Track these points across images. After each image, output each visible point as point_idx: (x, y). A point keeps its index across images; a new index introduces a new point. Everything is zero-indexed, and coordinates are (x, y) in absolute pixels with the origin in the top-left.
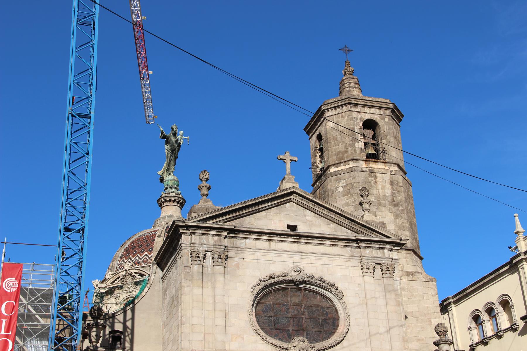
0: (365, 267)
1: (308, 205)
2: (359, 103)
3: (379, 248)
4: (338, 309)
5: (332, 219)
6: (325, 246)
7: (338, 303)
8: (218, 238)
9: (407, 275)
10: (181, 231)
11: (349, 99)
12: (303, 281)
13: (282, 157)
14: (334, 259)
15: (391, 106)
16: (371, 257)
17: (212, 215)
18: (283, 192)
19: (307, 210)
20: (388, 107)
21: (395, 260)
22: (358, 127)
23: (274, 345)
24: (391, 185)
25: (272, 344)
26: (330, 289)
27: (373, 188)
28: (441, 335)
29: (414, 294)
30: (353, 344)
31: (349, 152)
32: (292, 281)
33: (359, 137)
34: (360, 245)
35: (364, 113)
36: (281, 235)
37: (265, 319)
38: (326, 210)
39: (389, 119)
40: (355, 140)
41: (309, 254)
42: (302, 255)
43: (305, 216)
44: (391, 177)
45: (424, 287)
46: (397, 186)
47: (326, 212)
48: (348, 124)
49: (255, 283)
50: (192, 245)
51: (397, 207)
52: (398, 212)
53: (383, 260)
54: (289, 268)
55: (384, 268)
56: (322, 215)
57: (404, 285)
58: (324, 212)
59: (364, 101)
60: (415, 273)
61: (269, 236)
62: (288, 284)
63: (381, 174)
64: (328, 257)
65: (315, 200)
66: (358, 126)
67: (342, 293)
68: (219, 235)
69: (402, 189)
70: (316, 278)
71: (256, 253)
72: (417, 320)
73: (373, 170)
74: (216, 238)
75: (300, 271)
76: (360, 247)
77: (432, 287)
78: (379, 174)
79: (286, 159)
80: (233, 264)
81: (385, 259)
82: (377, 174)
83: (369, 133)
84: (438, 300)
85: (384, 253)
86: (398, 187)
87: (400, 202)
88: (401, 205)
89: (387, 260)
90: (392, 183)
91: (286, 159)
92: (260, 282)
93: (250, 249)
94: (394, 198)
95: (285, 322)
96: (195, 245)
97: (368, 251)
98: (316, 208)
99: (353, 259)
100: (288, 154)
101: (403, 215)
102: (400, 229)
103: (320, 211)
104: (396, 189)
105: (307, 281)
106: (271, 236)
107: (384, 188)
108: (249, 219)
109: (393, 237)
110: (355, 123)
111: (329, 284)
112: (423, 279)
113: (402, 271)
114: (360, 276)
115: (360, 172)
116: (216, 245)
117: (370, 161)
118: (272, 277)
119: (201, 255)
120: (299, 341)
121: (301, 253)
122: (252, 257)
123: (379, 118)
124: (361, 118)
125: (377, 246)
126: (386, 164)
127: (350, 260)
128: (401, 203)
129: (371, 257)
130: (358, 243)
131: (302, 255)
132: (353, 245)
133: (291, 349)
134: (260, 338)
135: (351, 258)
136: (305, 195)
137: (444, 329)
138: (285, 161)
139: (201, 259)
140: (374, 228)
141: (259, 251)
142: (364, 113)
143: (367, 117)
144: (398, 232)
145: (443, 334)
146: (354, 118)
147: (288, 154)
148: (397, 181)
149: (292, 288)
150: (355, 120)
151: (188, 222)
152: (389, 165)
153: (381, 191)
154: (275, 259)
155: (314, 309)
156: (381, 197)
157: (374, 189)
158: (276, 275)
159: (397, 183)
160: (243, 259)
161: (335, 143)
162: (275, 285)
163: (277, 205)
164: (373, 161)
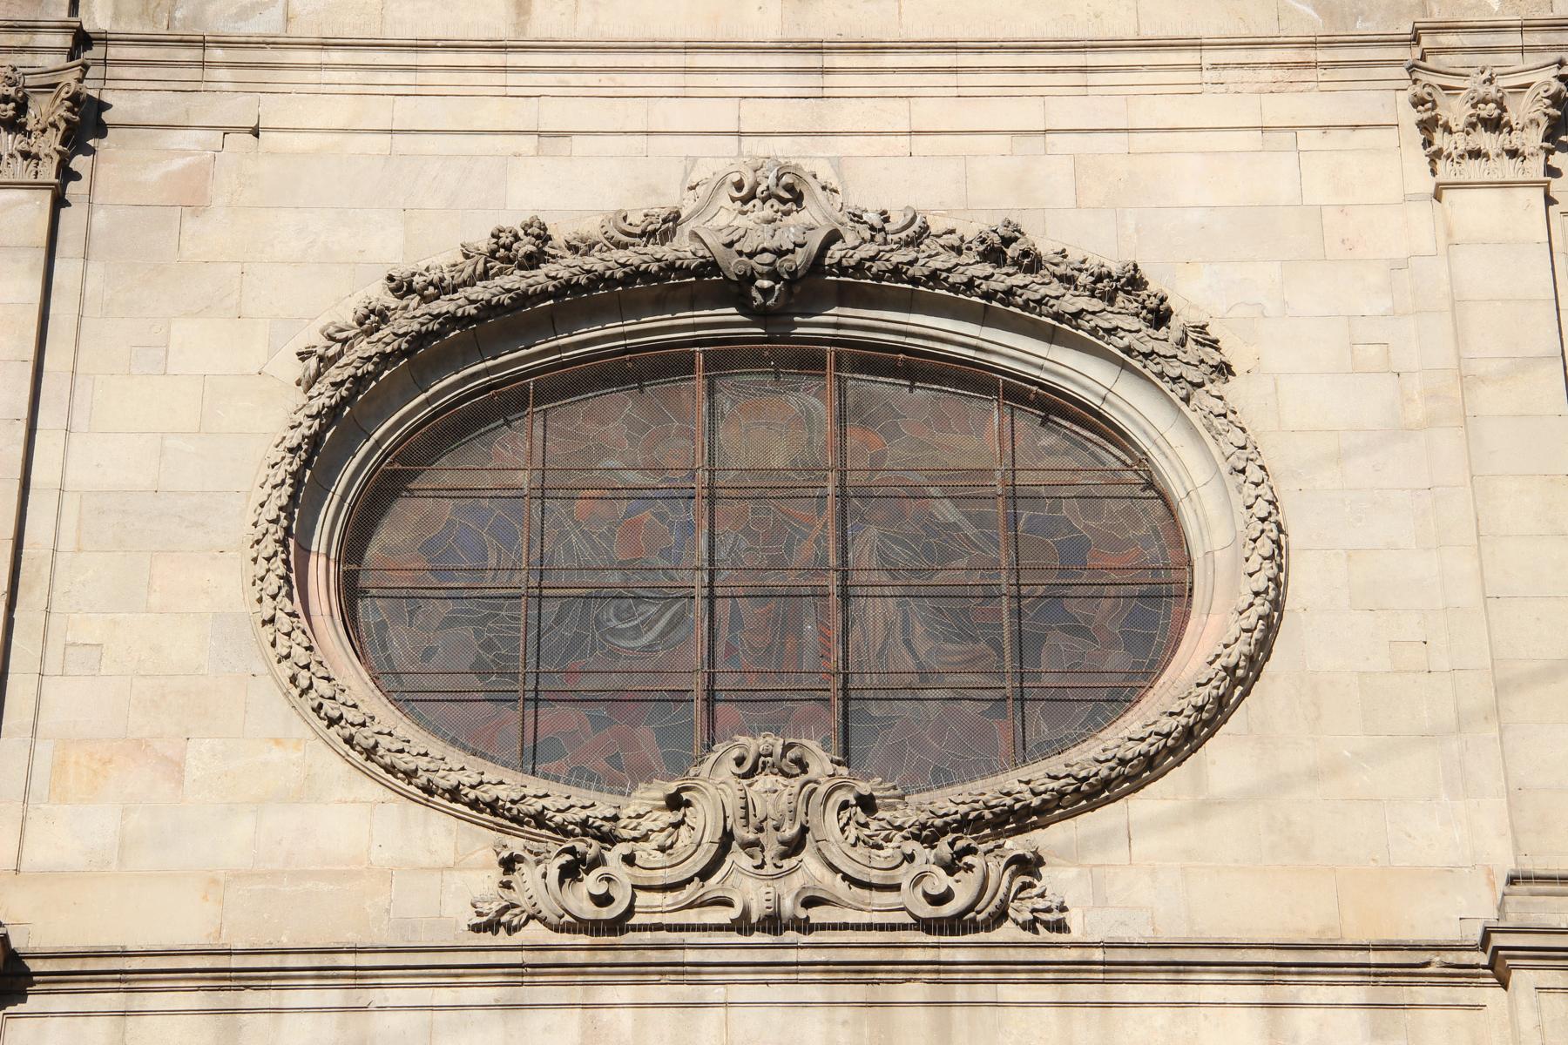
0: (1455, 111)
4: (1177, 490)
7: (1175, 436)
12: (817, 264)
16: (1523, 28)
23: (474, 804)
25: (454, 794)
26: (1078, 315)
30: (1315, 775)
37: (449, 622)
41: (889, 60)
42: (824, 71)
49: (346, 316)
62: (686, 317)
64: (1083, 69)
67: (1214, 344)
70: (953, 240)
71: (384, 77)
75: (790, 188)
80: (153, 175)
92: (392, 301)
93: (324, 45)
99: (1335, 65)
105: (859, 268)
111: (1083, 279)
114: (1407, 198)
118: (502, 253)
120: (740, 761)
121: (818, 49)
122: (339, 111)
129: (1523, 28)
131: (824, 71)
133: (646, 824)
134: (346, 758)
154: (554, 115)
155: (947, 511)
158: (560, 234)
160: (255, 132)
162: (554, 322)
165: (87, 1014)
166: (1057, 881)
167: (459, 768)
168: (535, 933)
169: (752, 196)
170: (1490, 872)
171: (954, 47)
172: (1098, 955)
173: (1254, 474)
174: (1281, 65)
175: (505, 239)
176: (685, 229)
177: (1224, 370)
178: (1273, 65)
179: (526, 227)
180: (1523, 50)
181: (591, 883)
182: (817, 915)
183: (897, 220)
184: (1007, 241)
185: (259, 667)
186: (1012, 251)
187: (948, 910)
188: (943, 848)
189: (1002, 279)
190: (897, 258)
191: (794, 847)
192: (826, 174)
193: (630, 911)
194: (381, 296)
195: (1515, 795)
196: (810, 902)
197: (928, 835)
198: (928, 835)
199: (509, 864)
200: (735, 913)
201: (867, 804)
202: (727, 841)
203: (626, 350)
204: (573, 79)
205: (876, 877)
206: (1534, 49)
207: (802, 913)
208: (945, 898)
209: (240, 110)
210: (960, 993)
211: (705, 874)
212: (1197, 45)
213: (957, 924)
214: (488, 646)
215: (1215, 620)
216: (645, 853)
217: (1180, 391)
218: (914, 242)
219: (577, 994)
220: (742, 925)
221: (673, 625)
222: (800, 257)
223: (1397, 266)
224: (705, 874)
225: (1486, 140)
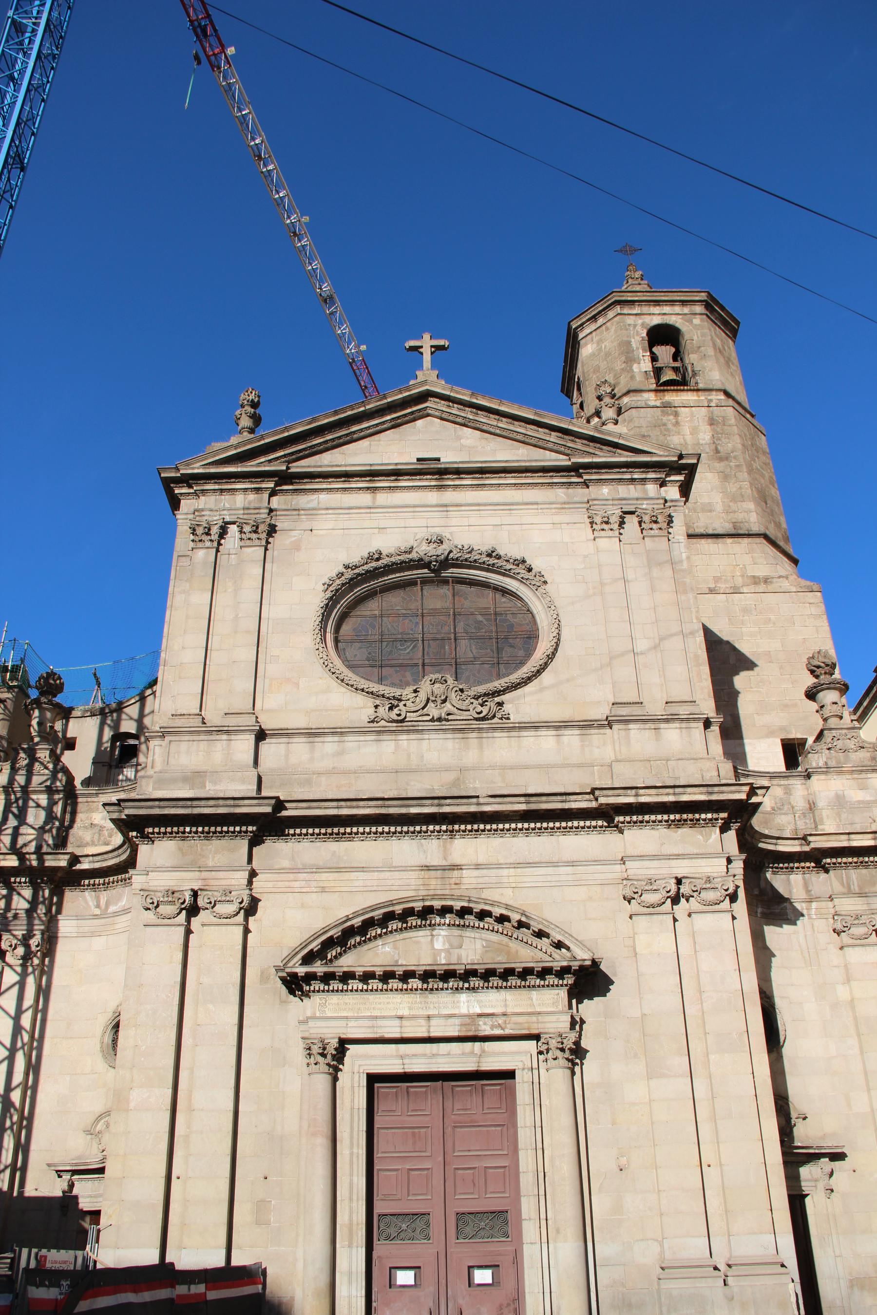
0: (598, 520)
1: (463, 415)
2: (636, 299)
3: (633, 480)
4: (535, 612)
5: (519, 437)
6: (504, 490)
7: (534, 599)
8: (256, 495)
9: (755, 583)
10: (176, 492)
11: (614, 294)
12: (447, 558)
13: (413, 343)
14: (526, 511)
15: (703, 296)
17: (239, 450)
18: (401, 393)
19: (465, 428)
20: (697, 298)
21: (672, 501)
22: (638, 339)
23: (367, 693)
24: (711, 424)
25: (363, 690)
26: (510, 570)
27: (672, 433)
28: (819, 674)
29: (772, 617)
30: (568, 680)
31: (622, 382)
32: (421, 563)
33: (641, 355)
34: (586, 477)
35: (650, 314)
36: (397, 473)
37: (360, 648)
38: (504, 419)
39: (702, 320)
40: (630, 360)
41: (463, 508)
42: (447, 511)
43: (459, 438)
44: (708, 411)
45: (793, 603)
46: (724, 425)
47: (504, 423)
48: (618, 336)
49: (334, 574)
50: (196, 513)
51: (726, 462)
52: (729, 470)
53: (642, 504)
54: (416, 538)
55: (646, 518)
56: (498, 431)
57: (748, 603)
58: (500, 425)
59: (645, 294)
60: (773, 578)
61: (370, 481)
62: (415, 572)
63: (687, 409)
64: (510, 510)
65: (475, 401)
66: (638, 338)
68: (258, 490)
69: (735, 430)
70: (480, 552)
71: (341, 516)
72: (781, 668)
73: (669, 403)
74: (252, 496)
75: (440, 540)
76: (586, 484)
77: (812, 601)
78: (682, 409)
79: (422, 347)
80: (288, 542)
81: (648, 502)
82: (679, 409)
83: (665, 352)
84: (827, 624)
85: (645, 491)
86: (726, 427)
87: (732, 452)
88: (735, 458)
89: (652, 502)
90: (712, 422)
91: (422, 347)
92: (344, 570)
93: (327, 509)
94: (719, 447)
95: (408, 651)
96: (203, 513)
97: (605, 491)
98: (482, 417)
99: (570, 508)
100: (427, 336)
101: (739, 475)
102: (734, 499)
103: (491, 423)
104: (722, 430)
105: (457, 559)
106: (374, 481)
107: (694, 431)
108: (330, 456)
109: (661, 453)
110: (632, 332)
111: (511, 561)
112: (792, 587)
113: (743, 576)
115: (642, 409)
116: (248, 509)
117: (664, 391)
118: (370, 558)
119: (215, 530)
120: (431, 681)
121: (446, 506)
123: (680, 321)
124: (643, 325)
125: (628, 476)
126: (700, 393)
127: (563, 511)
128: (735, 453)
130: (580, 476)
131: (447, 511)
132: (569, 480)
133: (409, 697)
134: (337, 682)
135: (566, 506)
136: (452, 394)
137: (824, 660)
138: (421, 350)
139: (215, 537)
140: (616, 440)
141: (347, 511)
142: (650, 314)
143: (656, 321)
144: (729, 506)
145: (823, 672)
146: (629, 325)
147: (427, 336)
148: (723, 417)
149: (425, 581)
150: (631, 328)
151: (185, 469)
152: (707, 393)
153: (689, 438)
155: (480, 618)
156: (690, 447)
157: (673, 435)
158: (384, 553)
159: (724, 421)
160: (311, 530)
161: (597, 377)
162: (383, 574)
163: (396, 425)
164: (671, 390)
165: (280, 743)
166: (507, 708)
167: (363, 684)
168: (383, 723)
169: (431, 542)
170: (608, 702)
171: (479, 505)
172: (517, 725)
173: (553, 608)
174: (557, 508)
175: (371, 554)
176: (414, 551)
177: (545, 582)
178: (555, 508)
179: (376, 551)
180: (613, 505)
181: (396, 711)
182: (450, 717)
183: (466, 547)
184: (493, 552)
185: (315, 660)
186: (494, 554)
187: (481, 715)
188: (480, 701)
189: (492, 561)
190: (466, 557)
191: (444, 701)
192: (448, 536)
193: (405, 717)
194: (341, 569)
195: (614, 684)
196: (449, 714)
197: (476, 698)
198: (476, 698)
199: (376, 707)
200: (430, 717)
201: (462, 690)
202: (428, 700)
203: (401, 580)
204: (387, 515)
205: (464, 708)
206: (616, 505)
207: (447, 717)
208: (479, 713)
209: (307, 525)
210: (485, 735)
211: (423, 708)
212: (537, 504)
213: (483, 719)
214: (370, 653)
215: (544, 643)
216: (409, 703)
217: (535, 587)
218: (470, 552)
219: (393, 737)
220: (432, 720)
221: (414, 647)
222: (442, 557)
223: (585, 557)
224: (423, 708)
225: (605, 526)
